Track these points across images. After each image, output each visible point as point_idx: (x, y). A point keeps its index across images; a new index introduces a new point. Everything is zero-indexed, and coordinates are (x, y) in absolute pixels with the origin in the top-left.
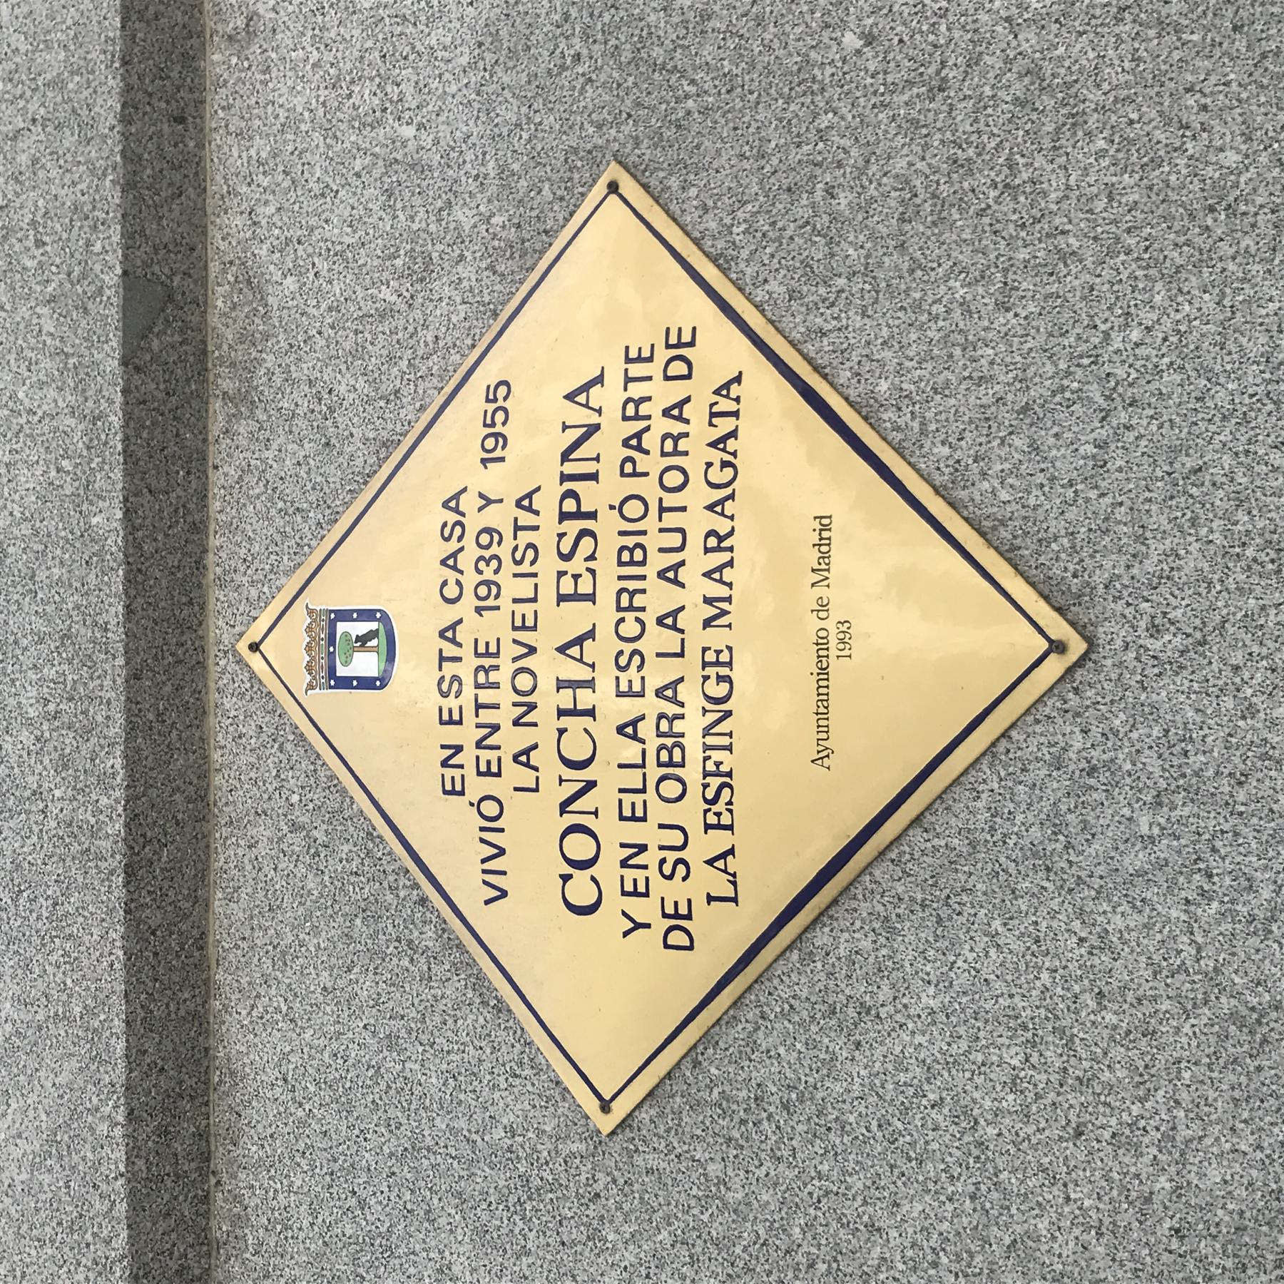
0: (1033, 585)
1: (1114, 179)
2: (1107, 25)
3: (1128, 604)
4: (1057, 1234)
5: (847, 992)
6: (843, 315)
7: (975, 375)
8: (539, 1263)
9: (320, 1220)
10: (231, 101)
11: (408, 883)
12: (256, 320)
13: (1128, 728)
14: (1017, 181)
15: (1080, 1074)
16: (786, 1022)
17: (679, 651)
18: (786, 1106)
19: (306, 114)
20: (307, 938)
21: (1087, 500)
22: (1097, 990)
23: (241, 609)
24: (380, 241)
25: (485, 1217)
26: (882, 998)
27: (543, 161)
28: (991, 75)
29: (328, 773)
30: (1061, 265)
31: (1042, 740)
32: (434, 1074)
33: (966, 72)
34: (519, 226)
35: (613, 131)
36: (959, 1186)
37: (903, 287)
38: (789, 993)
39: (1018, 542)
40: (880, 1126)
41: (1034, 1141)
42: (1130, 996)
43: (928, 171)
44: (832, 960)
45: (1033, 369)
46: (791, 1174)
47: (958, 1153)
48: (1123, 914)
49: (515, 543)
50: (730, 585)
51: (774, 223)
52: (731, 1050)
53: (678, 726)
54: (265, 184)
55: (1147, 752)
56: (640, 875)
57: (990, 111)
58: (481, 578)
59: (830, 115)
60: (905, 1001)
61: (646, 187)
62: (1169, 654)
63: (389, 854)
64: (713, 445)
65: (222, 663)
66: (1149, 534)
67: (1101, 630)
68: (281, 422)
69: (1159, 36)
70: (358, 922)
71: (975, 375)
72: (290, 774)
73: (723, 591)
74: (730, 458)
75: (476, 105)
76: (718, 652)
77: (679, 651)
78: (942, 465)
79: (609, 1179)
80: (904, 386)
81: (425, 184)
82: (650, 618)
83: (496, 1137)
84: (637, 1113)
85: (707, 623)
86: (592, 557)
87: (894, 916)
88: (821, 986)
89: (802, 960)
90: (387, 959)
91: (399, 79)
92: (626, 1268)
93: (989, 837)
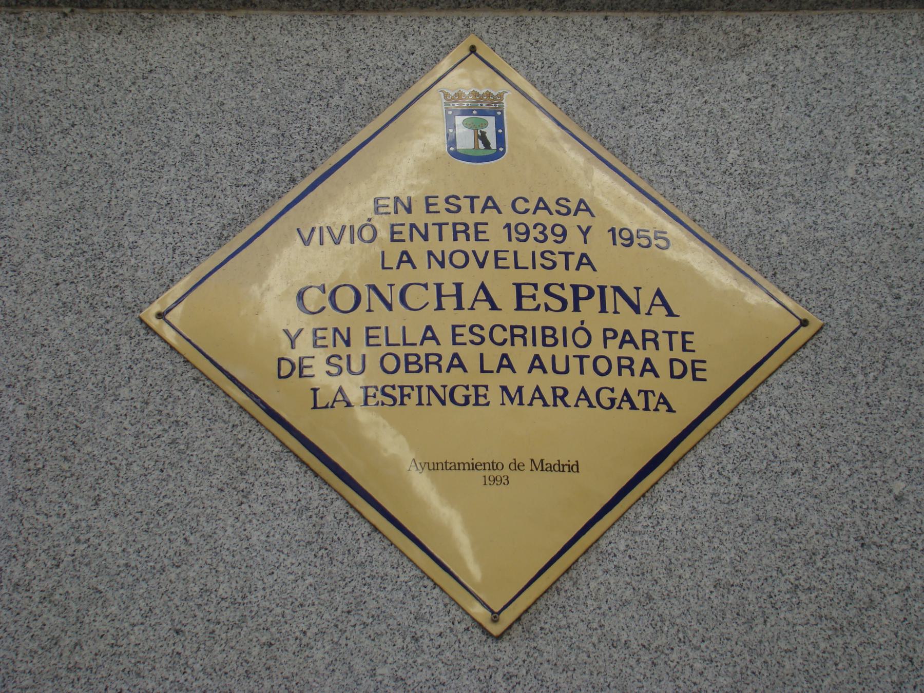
0: (535, 603)
1: (799, 654)
2: (901, 651)
3: (524, 661)
4: (109, 619)
5: (256, 483)
6: (713, 481)
7: (672, 566)
8: (41, 267)
9: (48, 98)
10: (881, 30)
11: (305, 169)
12: (716, 51)
13: (445, 661)
14: (799, 593)
15: (217, 632)
16: (232, 442)
17: (485, 369)
18: (174, 441)
19: (868, 92)
20: (259, 90)
21: (591, 636)
22: (273, 642)
23: (500, 38)
24: (772, 149)
25: (69, 227)
26: (255, 505)
27: (825, 273)
28: (871, 577)
29: (382, 108)
30: (744, 620)
31: (434, 609)
32: (168, 188)
33: (873, 561)
34: (779, 254)
35: (844, 323)
36: (134, 556)
37: (731, 520)
38: (252, 444)
39: (562, 593)
40: (168, 505)
41: (170, 603)
42: (271, 663)
43: (808, 536)
44: (277, 472)
45: (676, 603)
46: (128, 444)
47: (156, 555)
48: (323, 658)
49: (556, 252)
50: (531, 404)
51: (776, 434)
52: (209, 404)
53: (433, 368)
54: (817, 58)
55: (429, 672)
56: (329, 341)
57: (847, 576)
58: (531, 228)
59: (848, 473)
60: (254, 521)
61: (804, 346)
62: (494, 686)
63: (326, 155)
64: (626, 393)
65: (460, 23)
66: (570, 673)
67: (507, 644)
68: (640, 71)
69: (892, 682)
70: (274, 131)
71: (672, 566)
72: (380, 77)
73: (526, 399)
74: (617, 404)
75: (867, 223)
76: (485, 396)
77: (485, 369)
78: (612, 545)
79: (109, 318)
80: (665, 521)
81: (812, 184)
82: (507, 349)
83: (128, 235)
84: (157, 338)
85: (504, 389)
86: (547, 308)
87: (310, 514)
88: (259, 465)
89: (275, 453)
90: (249, 153)
91: (890, 164)
92: (46, 330)
93: (367, 575)
